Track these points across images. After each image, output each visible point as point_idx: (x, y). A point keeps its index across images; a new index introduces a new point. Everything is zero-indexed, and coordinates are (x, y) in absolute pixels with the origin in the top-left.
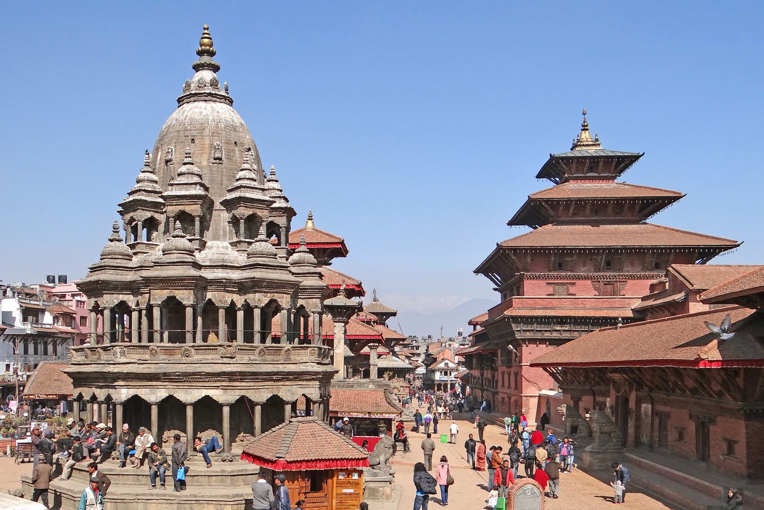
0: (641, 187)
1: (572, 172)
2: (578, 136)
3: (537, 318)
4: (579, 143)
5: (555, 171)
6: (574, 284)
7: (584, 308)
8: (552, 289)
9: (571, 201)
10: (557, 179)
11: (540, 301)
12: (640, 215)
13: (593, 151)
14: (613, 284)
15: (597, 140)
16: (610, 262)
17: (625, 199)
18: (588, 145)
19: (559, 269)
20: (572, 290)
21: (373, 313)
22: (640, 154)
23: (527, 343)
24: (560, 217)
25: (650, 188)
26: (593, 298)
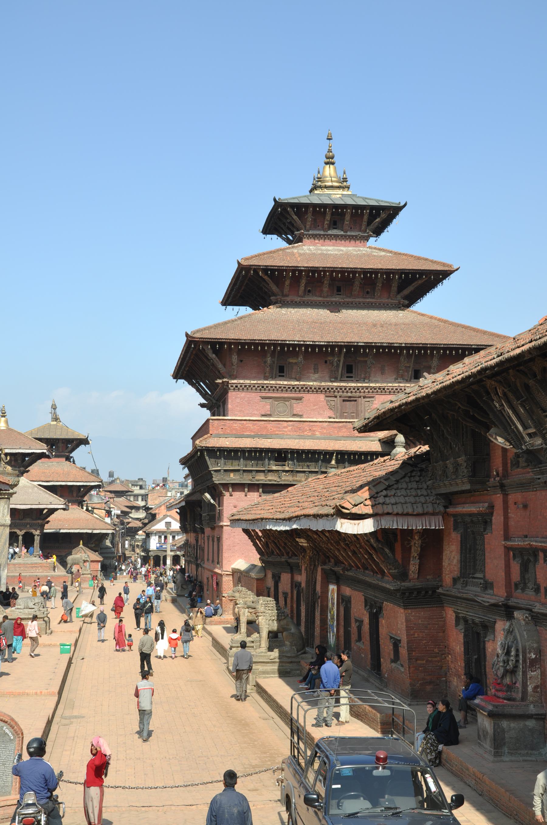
0: (400, 254)
1: (308, 227)
2: (319, 173)
3: (243, 451)
4: (319, 183)
5: (284, 224)
6: (300, 399)
7: (313, 437)
8: (268, 407)
9: (301, 271)
10: (289, 236)
11: (250, 424)
12: (399, 297)
13: (338, 196)
14: (356, 401)
15: (345, 180)
16: (351, 366)
17: (375, 272)
18: (332, 187)
19: (280, 376)
20: (298, 407)
21: (40, 440)
22: (402, 204)
23: (231, 490)
24: (287, 296)
25: (412, 256)
26: (326, 422)
